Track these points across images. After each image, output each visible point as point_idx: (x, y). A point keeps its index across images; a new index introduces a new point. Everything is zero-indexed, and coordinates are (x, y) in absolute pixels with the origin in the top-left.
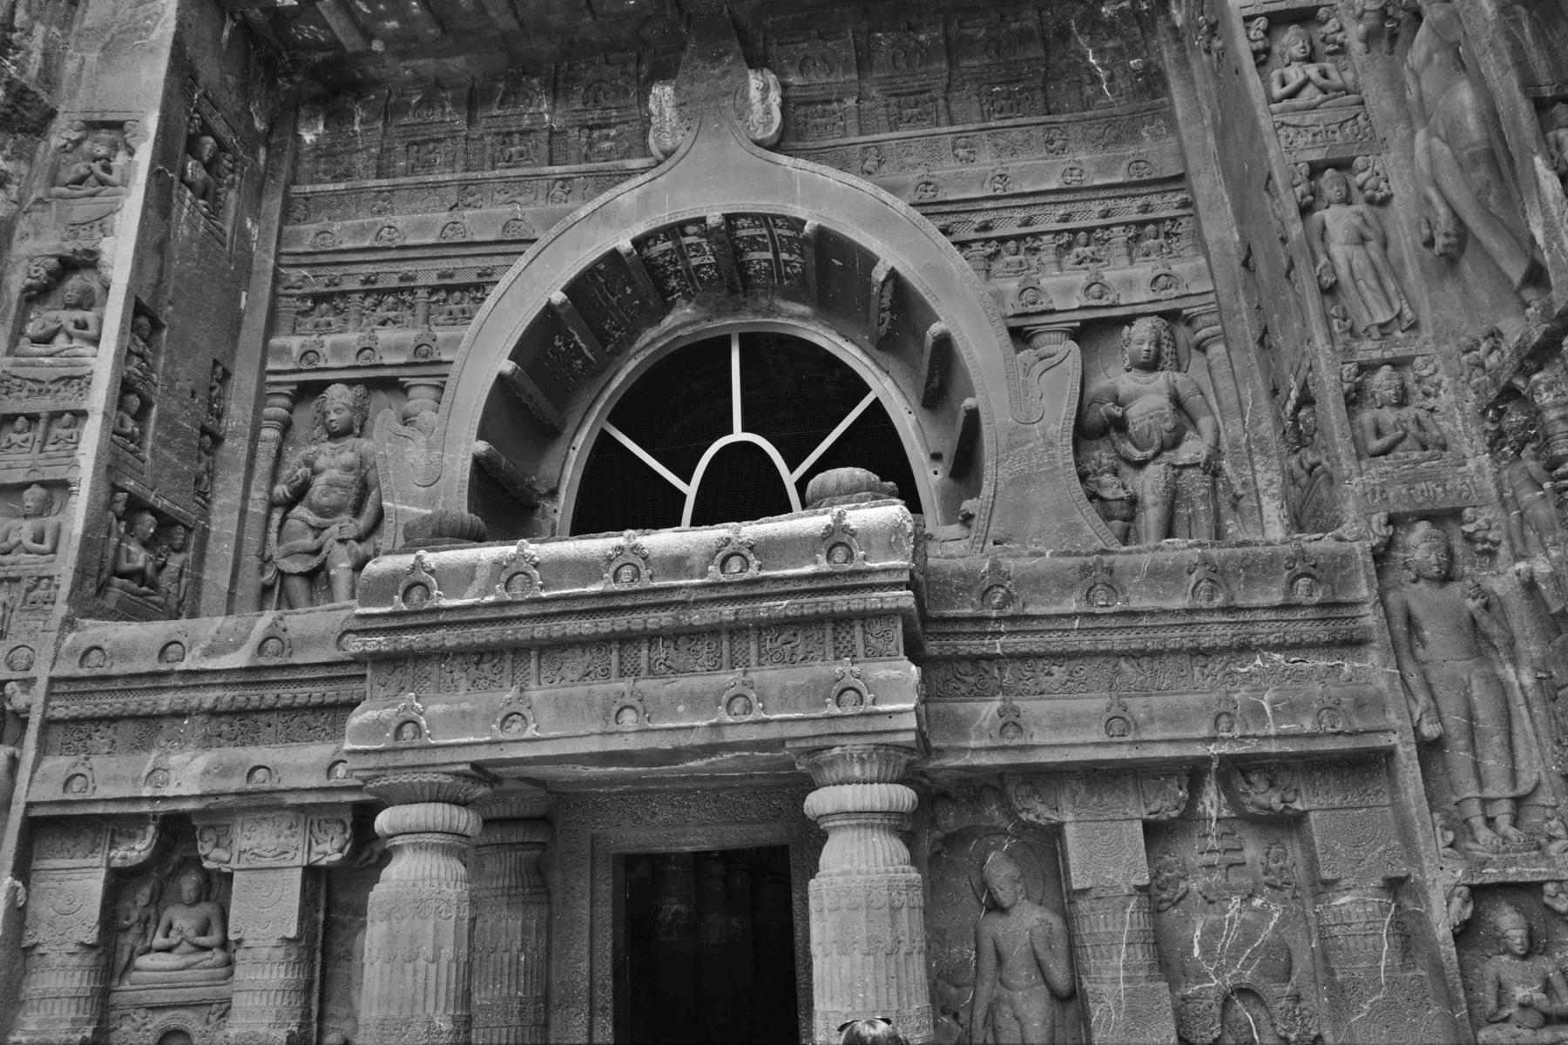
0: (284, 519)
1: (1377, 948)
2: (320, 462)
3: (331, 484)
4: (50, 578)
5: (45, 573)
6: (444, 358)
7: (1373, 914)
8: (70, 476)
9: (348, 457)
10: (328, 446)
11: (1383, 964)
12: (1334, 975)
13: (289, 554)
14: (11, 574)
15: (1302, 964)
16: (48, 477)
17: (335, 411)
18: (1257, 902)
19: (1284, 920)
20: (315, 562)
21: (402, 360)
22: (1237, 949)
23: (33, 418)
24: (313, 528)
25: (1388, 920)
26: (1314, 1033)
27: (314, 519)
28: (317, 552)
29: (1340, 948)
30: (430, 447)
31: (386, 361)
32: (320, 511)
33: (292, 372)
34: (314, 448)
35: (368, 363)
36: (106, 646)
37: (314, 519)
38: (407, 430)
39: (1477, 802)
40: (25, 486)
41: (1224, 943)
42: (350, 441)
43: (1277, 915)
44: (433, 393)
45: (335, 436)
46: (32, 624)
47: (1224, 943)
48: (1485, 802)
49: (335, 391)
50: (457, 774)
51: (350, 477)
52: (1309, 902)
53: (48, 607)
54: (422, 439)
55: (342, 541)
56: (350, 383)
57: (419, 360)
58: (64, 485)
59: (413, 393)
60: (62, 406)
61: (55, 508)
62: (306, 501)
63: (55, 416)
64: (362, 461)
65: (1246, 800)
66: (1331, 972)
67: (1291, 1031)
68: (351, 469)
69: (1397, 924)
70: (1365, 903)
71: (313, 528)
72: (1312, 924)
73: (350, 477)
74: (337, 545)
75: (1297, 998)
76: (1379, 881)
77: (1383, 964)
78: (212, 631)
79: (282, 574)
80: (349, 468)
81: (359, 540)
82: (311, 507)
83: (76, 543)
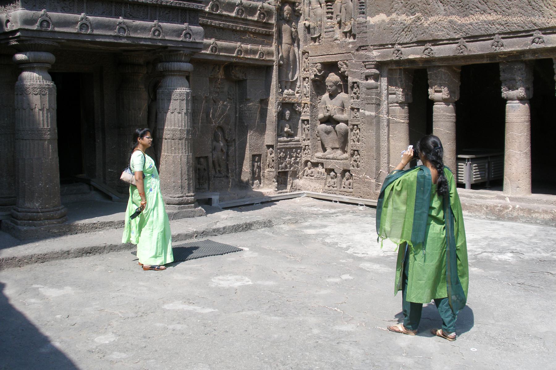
1: (256, 117)
18: (225, 103)
19: (230, 108)
22: (220, 115)
41: (217, 114)
47: (217, 114)
48: (287, 82)
50: (59, 43)
52: (238, 104)
65: (233, 75)
66: (244, 123)
69: (260, 111)
76: (258, 100)
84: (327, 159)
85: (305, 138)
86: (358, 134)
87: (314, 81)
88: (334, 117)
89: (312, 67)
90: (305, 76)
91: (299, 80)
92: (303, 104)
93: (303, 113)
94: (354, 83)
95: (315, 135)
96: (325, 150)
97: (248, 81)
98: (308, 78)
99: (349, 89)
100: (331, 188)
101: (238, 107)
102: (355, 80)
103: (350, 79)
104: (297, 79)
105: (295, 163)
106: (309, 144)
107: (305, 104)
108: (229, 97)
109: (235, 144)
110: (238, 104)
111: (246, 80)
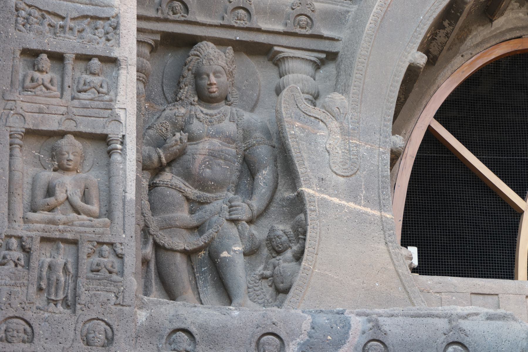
0: (152, 186)
2: (196, 126)
3: (213, 155)
4: (111, 244)
5: (106, 240)
6: (326, 33)
8: (110, 130)
9: (229, 127)
10: (200, 110)
13: (168, 226)
14: (69, 236)
16: (82, 128)
17: (214, 73)
20: (198, 241)
21: (280, 28)
23: (58, 58)
24: (188, 199)
27: (192, 192)
28: (198, 229)
30: (345, 133)
31: (264, 26)
32: (201, 184)
33: (157, 20)
34: (183, 111)
35: (241, 24)
36: (193, 329)
37: (192, 192)
38: (317, 112)
40: (61, 134)
42: (223, 108)
44: (309, 68)
45: (205, 98)
46: (103, 296)
49: (208, 49)
51: (231, 150)
53: (115, 277)
54: (334, 125)
55: (235, 221)
56: (220, 42)
57: (298, 30)
58: (103, 139)
59: (289, 65)
60: (88, 50)
61: (88, 164)
62: (176, 167)
63: (87, 58)
64: (247, 133)
68: (234, 141)
71: (188, 199)
73: (231, 150)
74: (226, 224)
78: (306, 326)
79: (157, 247)
80: (230, 140)
81: (250, 222)
82: (188, 176)
83: (132, 209)
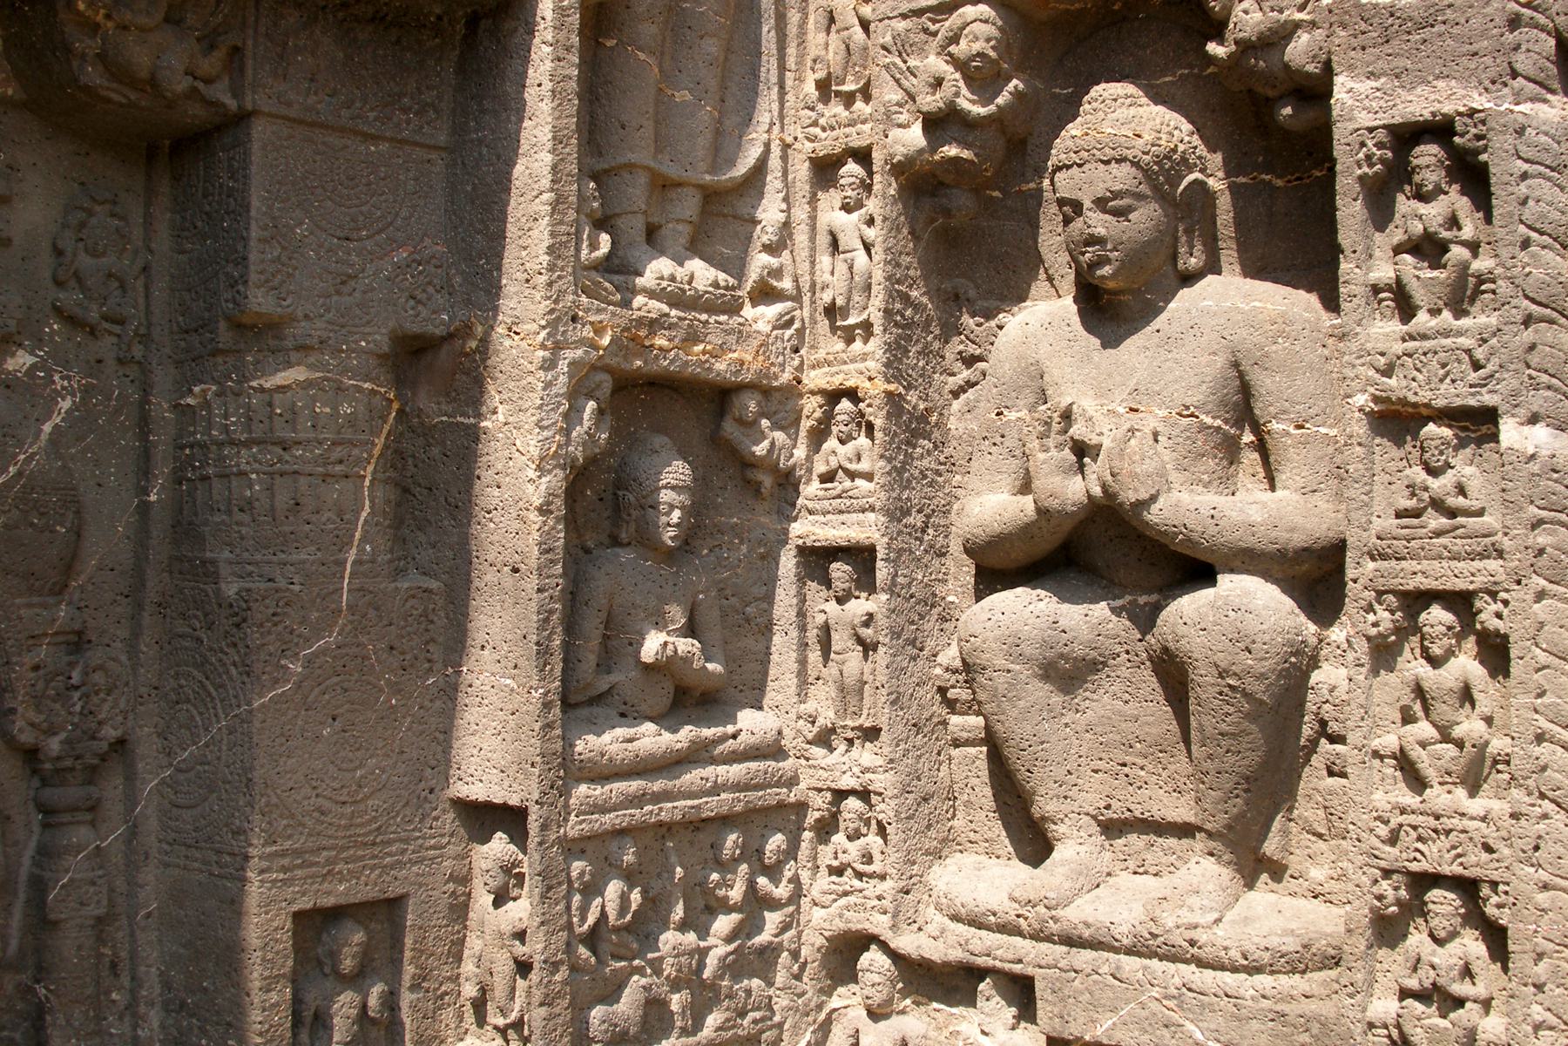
1: (345, 515)
7: (351, 421)
11: (352, 555)
12: (215, 578)
15: (108, 540)
19: (80, 422)
25: (380, 442)
26: (110, 733)
29: (248, 506)
39: (643, 179)
43: (66, 404)
48: (664, 186)
52: (163, 377)
65: (86, 45)
66: (208, 571)
67: (51, 731)
69: (396, 456)
70: (340, 389)
72: (161, 440)
75: (77, 642)
76: (380, 339)
77: (352, 555)
84: (1071, 941)
85: (827, 717)
86: (1466, 695)
87: (920, 184)
88: (1157, 515)
89: (902, 47)
90: (828, 144)
91: (773, 182)
92: (812, 406)
93: (811, 489)
94: (1406, 136)
95: (928, 694)
96: (1033, 842)
97: (259, 131)
98: (863, 156)
99: (1350, 211)
100: (848, 880)
101: (161, 408)
102: (1418, 105)
103: (1361, 104)
104: (760, 168)
105: (737, 966)
106: (879, 781)
107: (833, 396)
108: (71, 298)
109: (131, 800)
110: (163, 377)
111: (243, 118)
